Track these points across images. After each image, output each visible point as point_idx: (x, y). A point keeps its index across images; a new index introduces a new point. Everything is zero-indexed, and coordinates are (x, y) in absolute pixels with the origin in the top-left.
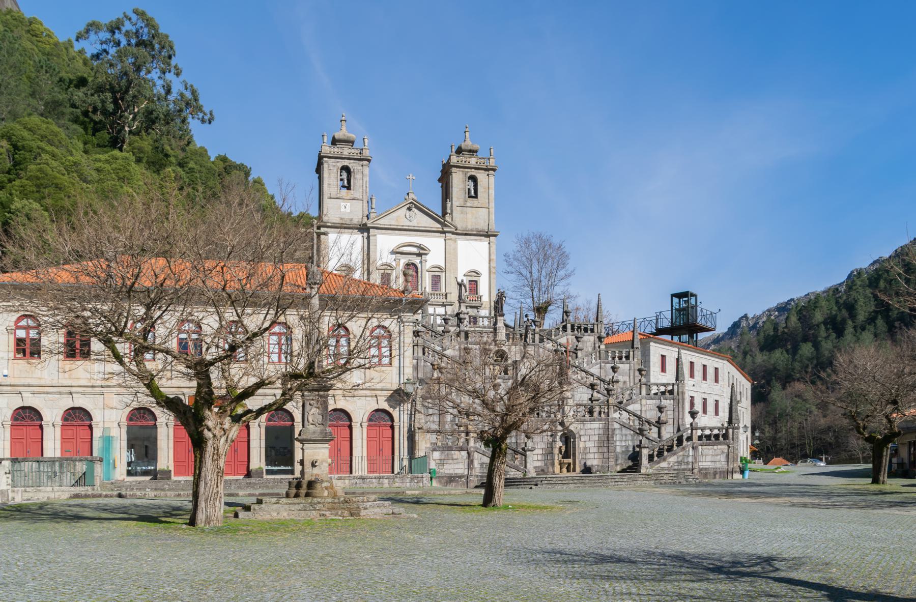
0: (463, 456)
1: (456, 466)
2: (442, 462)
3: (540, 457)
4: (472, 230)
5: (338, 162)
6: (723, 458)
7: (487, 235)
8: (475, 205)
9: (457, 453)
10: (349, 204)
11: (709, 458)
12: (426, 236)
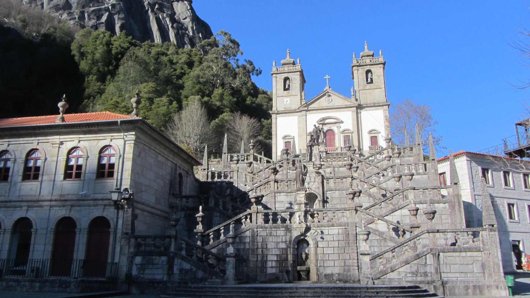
0: (163, 262)
1: (156, 271)
2: (142, 267)
3: (274, 264)
4: (370, 104)
5: (282, 76)
6: (477, 268)
7: (383, 106)
8: (371, 88)
9: (157, 258)
10: (289, 99)
12: (339, 111)
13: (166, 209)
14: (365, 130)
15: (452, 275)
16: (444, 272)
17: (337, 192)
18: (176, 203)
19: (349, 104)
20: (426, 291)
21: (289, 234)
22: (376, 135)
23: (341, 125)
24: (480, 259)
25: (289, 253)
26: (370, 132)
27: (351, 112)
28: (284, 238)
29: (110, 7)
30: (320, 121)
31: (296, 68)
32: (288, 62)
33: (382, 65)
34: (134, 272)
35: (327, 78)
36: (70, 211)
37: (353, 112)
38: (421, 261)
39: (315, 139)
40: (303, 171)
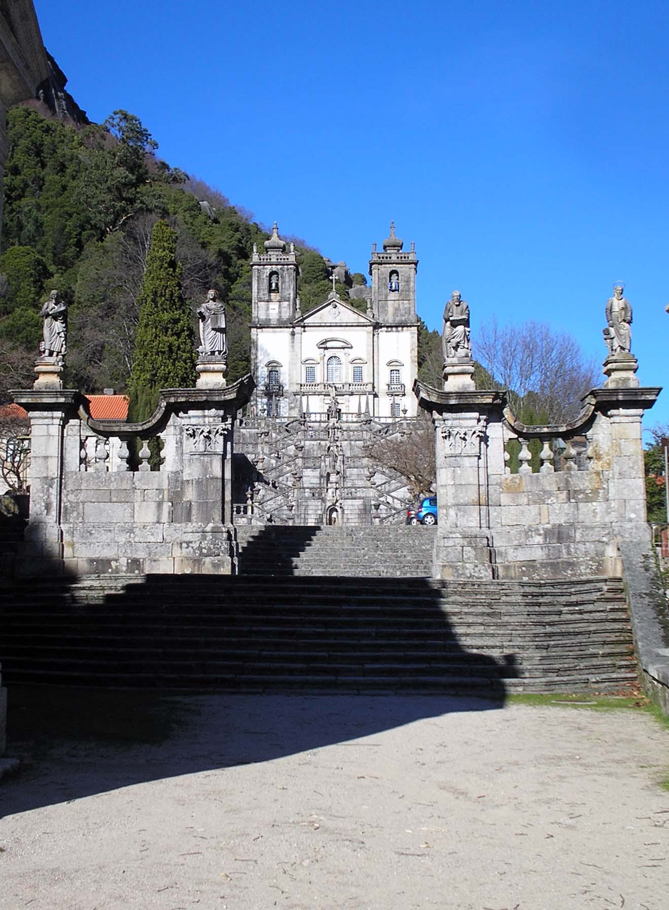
14: (384, 357)
17: (355, 469)
19: (363, 321)
21: (324, 504)
22: (397, 368)
26: (389, 364)
27: (365, 333)
30: (322, 344)
31: (288, 257)
32: (276, 245)
33: (413, 265)
35: (334, 278)
37: (368, 333)
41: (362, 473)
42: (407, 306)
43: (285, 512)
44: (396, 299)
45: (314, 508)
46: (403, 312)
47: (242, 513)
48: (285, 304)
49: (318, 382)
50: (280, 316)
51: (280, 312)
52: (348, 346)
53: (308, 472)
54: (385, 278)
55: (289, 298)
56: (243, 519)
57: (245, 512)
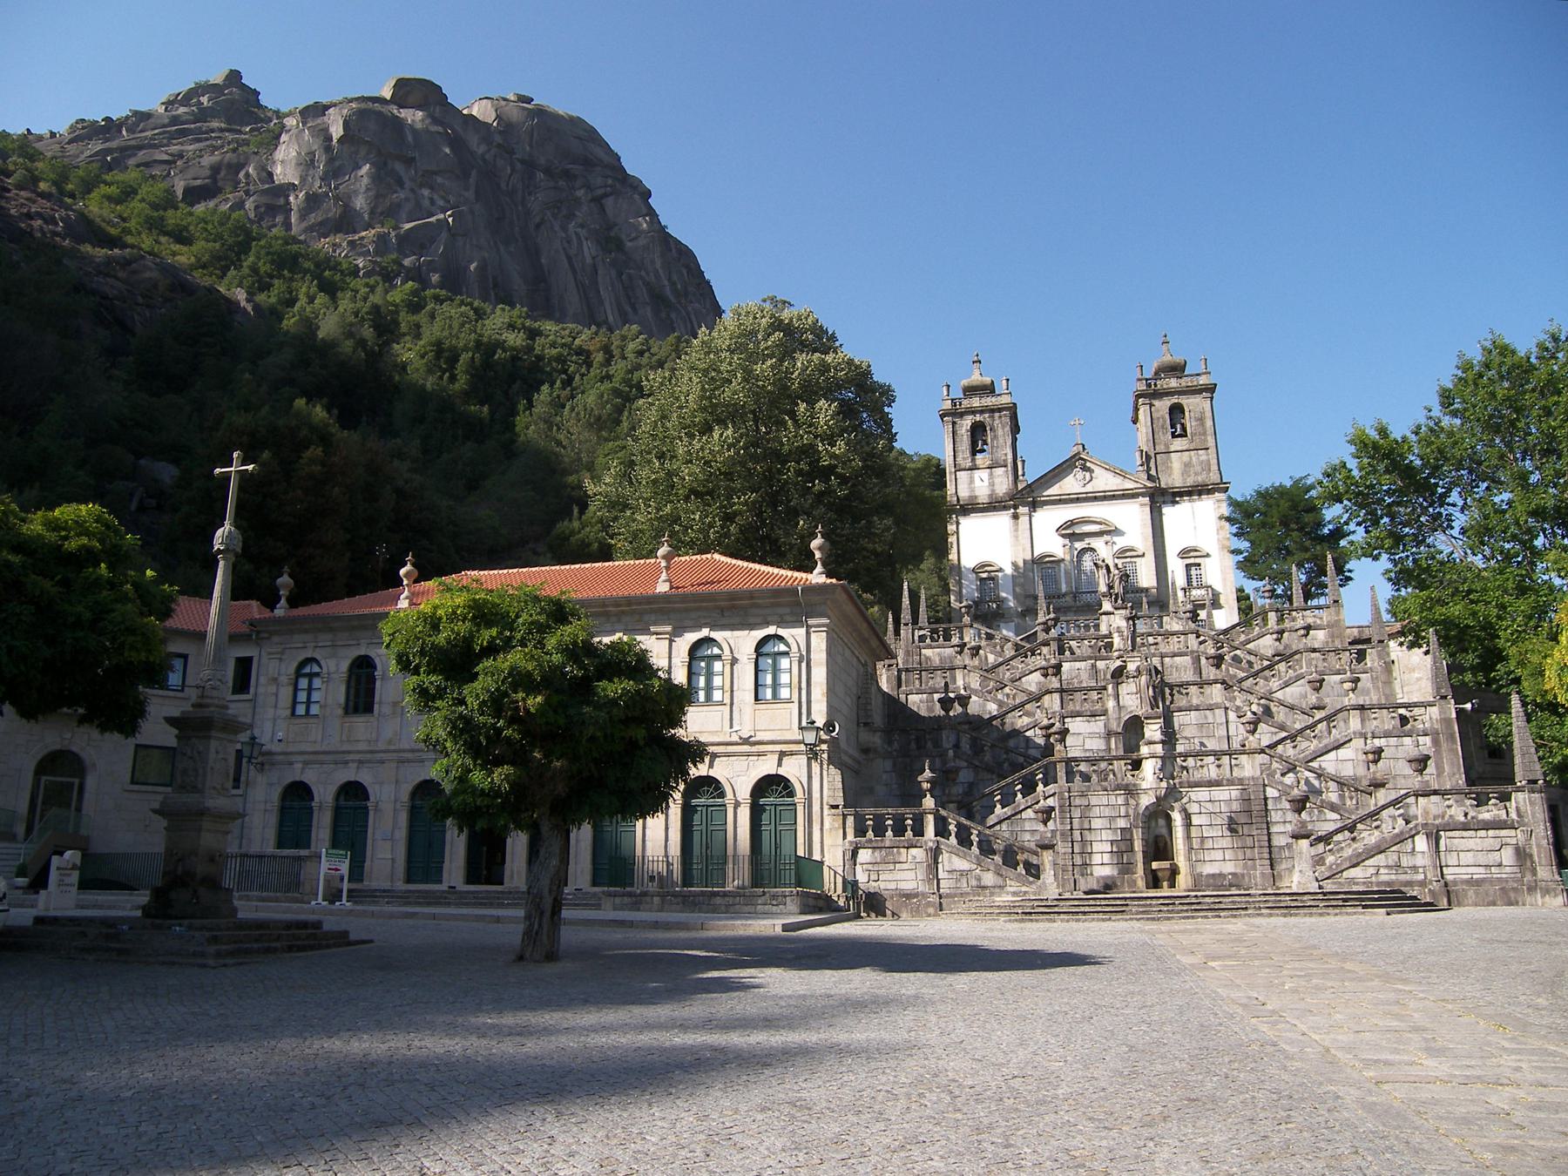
6: (1507, 856)
11: (1467, 858)
13: (856, 754)
14: (1173, 545)
15: (1463, 870)
16: (1447, 866)
18: (874, 743)
20: (1415, 898)
21: (1132, 802)
22: (1197, 561)
23: (1115, 539)
24: (1514, 841)
25: (1135, 837)
26: (1184, 553)
28: (1123, 809)
29: (450, 220)
34: (861, 877)
36: (780, 765)
38: (1408, 846)
39: (1117, 595)
40: (1154, 678)
41: (1211, 720)
42: (1204, 458)
43: (1028, 826)
44: (1184, 448)
45: (1107, 812)
46: (1198, 469)
47: (909, 833)
48: (1000, 471)
49: (1064, 588)
50: (993, 491)
51: (992, 484)
52: (1111, 532)
53: (1075, 725)
54: (1163, 417)
55: (1005, 461)
56: (913, 851)
57: (919, 831)
